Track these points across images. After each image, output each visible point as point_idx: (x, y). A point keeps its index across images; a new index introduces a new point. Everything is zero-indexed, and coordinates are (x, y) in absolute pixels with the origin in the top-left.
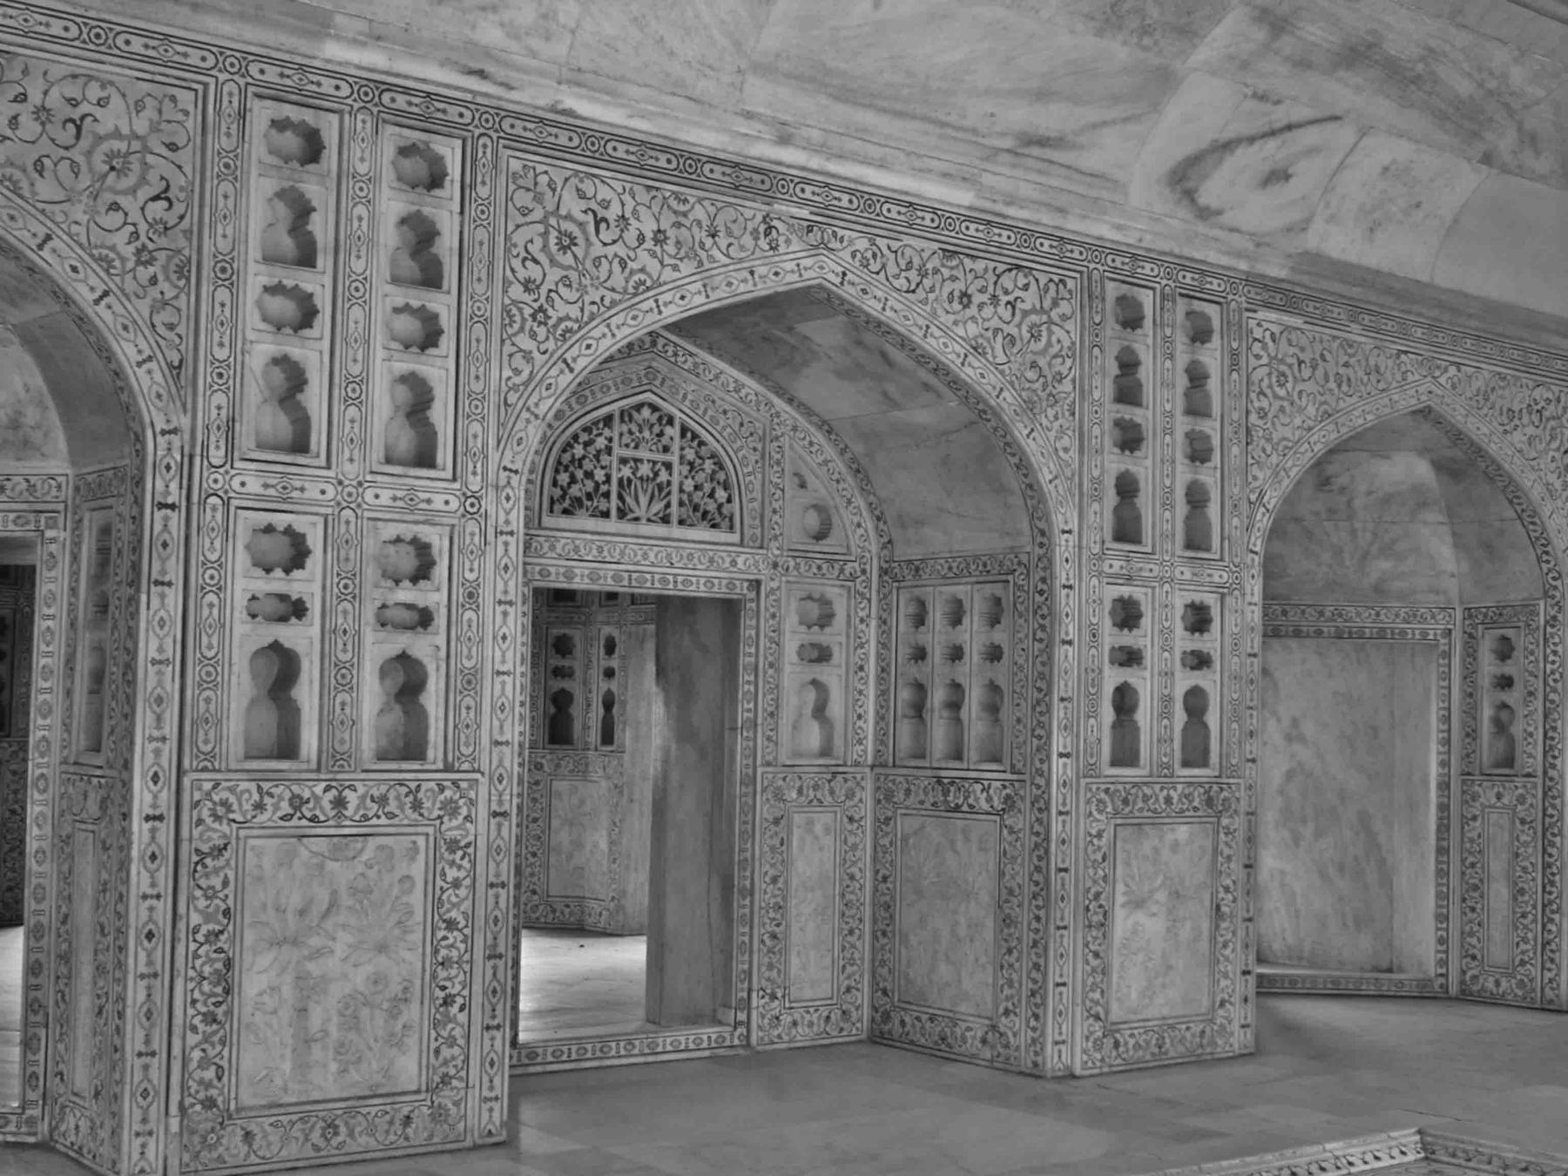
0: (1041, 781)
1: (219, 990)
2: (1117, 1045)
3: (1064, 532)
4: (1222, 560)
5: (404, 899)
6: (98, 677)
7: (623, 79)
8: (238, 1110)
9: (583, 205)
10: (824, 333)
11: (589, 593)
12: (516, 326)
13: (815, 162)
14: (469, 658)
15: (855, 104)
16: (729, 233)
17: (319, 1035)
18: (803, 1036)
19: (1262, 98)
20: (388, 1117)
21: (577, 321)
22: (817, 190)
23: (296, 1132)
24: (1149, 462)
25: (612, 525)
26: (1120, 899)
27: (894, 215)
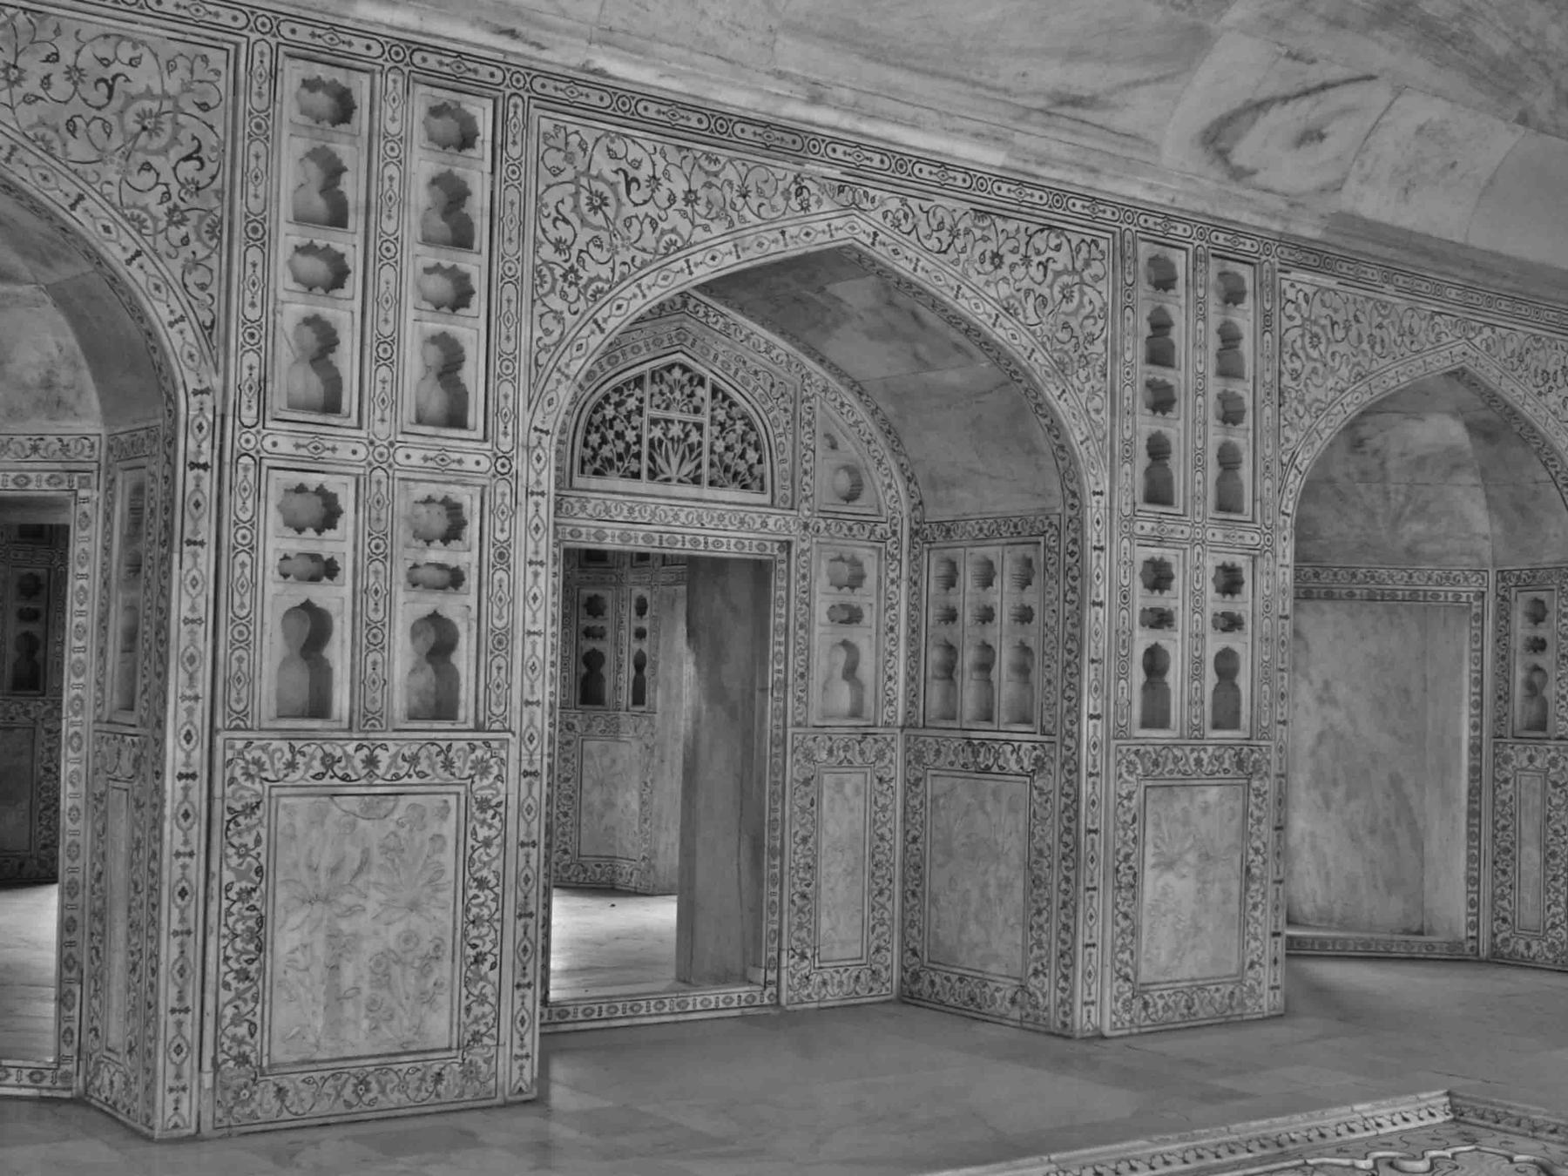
0: (1068, 741)
1: (252, 947)
2: (1146, 1005)
3: (1095, 493)
4: (1254, 521)
5: (435, 858)
6: (131, 636)
7: (652, 38)
8: (271, 1066)
9: (614, 165)
10: (855, 293)
11: (619, 554)
12: (547, 287)
13: (847, 122)
14: (500, 617)
15: (888, 64)
16: (760, 193)
17: (351, 993)
18: (833, 995)
19: (1295, 57)
20: (419, 1074)
21: (607, 281)
22: (849, 150)
23: (328, 1088)
24: (1180, 424)
25: (643, 486)
26: (1150, 860)
27: (925, 175)
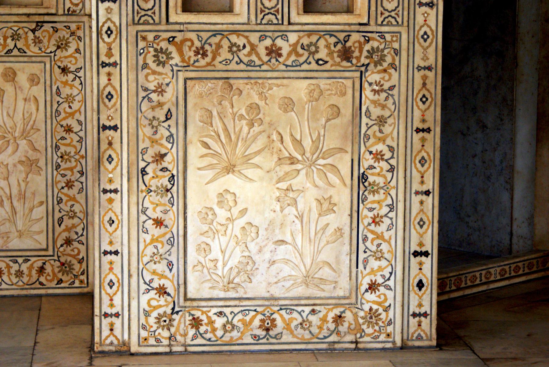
2: (196, 323)
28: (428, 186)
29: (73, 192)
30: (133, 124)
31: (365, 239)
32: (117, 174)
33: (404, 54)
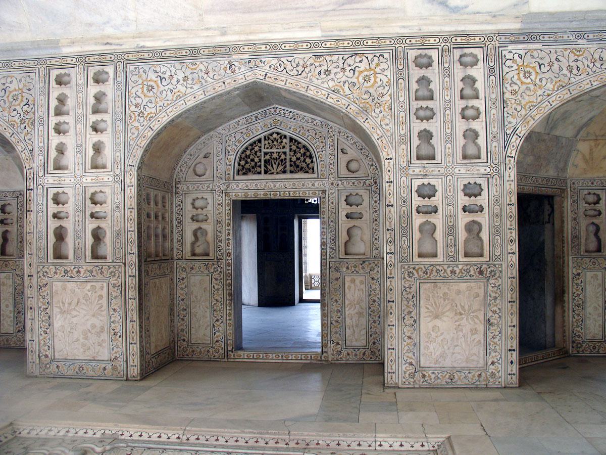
1: (47, 324)
3: (387, 159)
5: (100, 302)
9: (156, 75)
13: (243, 38)
16: (214, 71)
18: (352, 359)
28: (514, 324)
29: (376, 325)
30: (400, 300)
31: (490, 344)
32: (393, 319)
33: (503, 272)
